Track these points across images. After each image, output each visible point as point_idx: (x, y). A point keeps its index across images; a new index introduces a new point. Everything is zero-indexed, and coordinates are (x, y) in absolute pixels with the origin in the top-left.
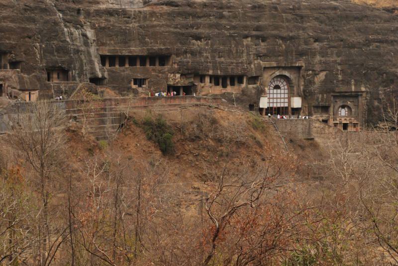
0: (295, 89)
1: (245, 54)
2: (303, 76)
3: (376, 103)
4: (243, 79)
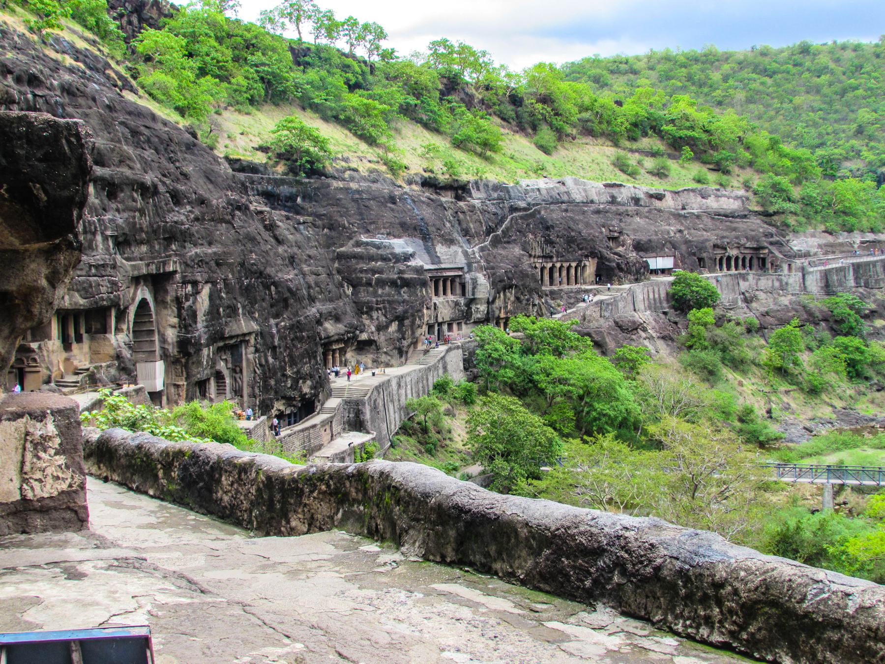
0: (156, 337)
1: (99, 238)
2: (178, 301)
3: (271, 360)
4: (111, 316)
